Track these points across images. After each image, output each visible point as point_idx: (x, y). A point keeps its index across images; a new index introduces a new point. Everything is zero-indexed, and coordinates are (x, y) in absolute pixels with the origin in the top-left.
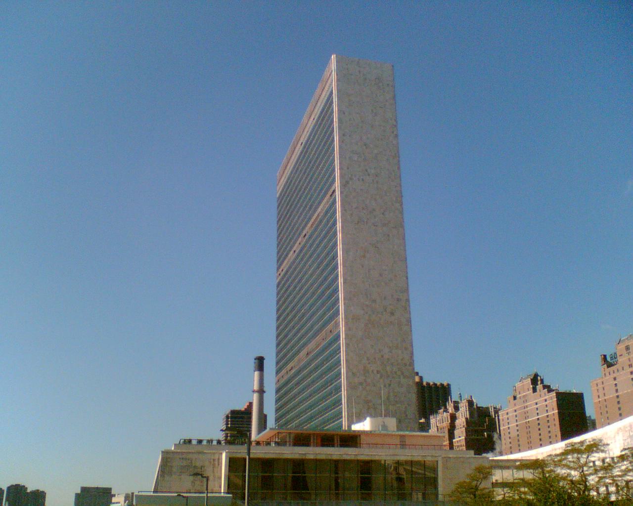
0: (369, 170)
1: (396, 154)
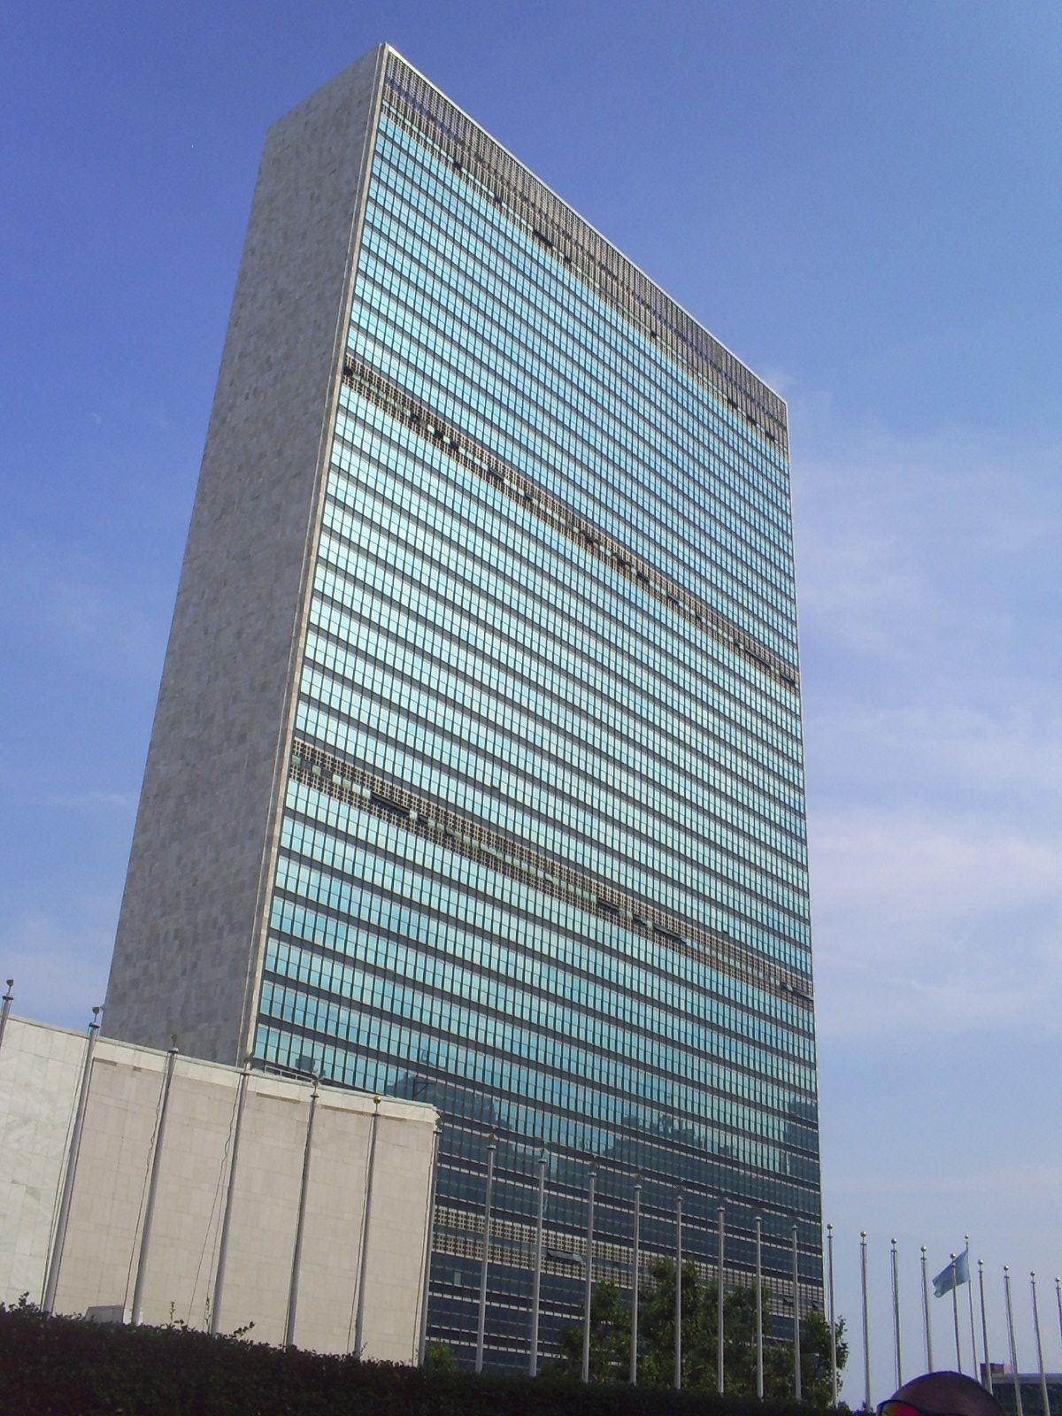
0: (272, 359)
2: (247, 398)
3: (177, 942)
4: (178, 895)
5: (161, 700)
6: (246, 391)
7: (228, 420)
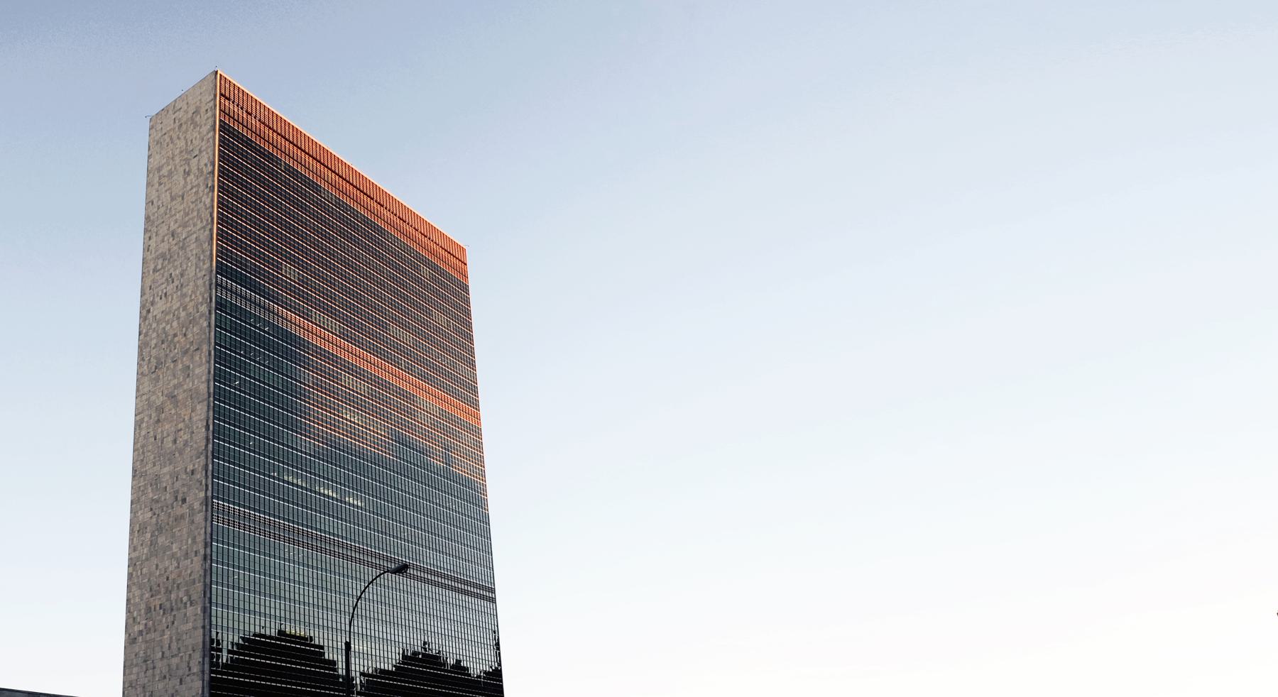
1: (207, 220)
2: (161, 298)
3: (162, 611)
4: (159, 586)
5: (134, 477)
6: (160, 294)
7: (151, 311)
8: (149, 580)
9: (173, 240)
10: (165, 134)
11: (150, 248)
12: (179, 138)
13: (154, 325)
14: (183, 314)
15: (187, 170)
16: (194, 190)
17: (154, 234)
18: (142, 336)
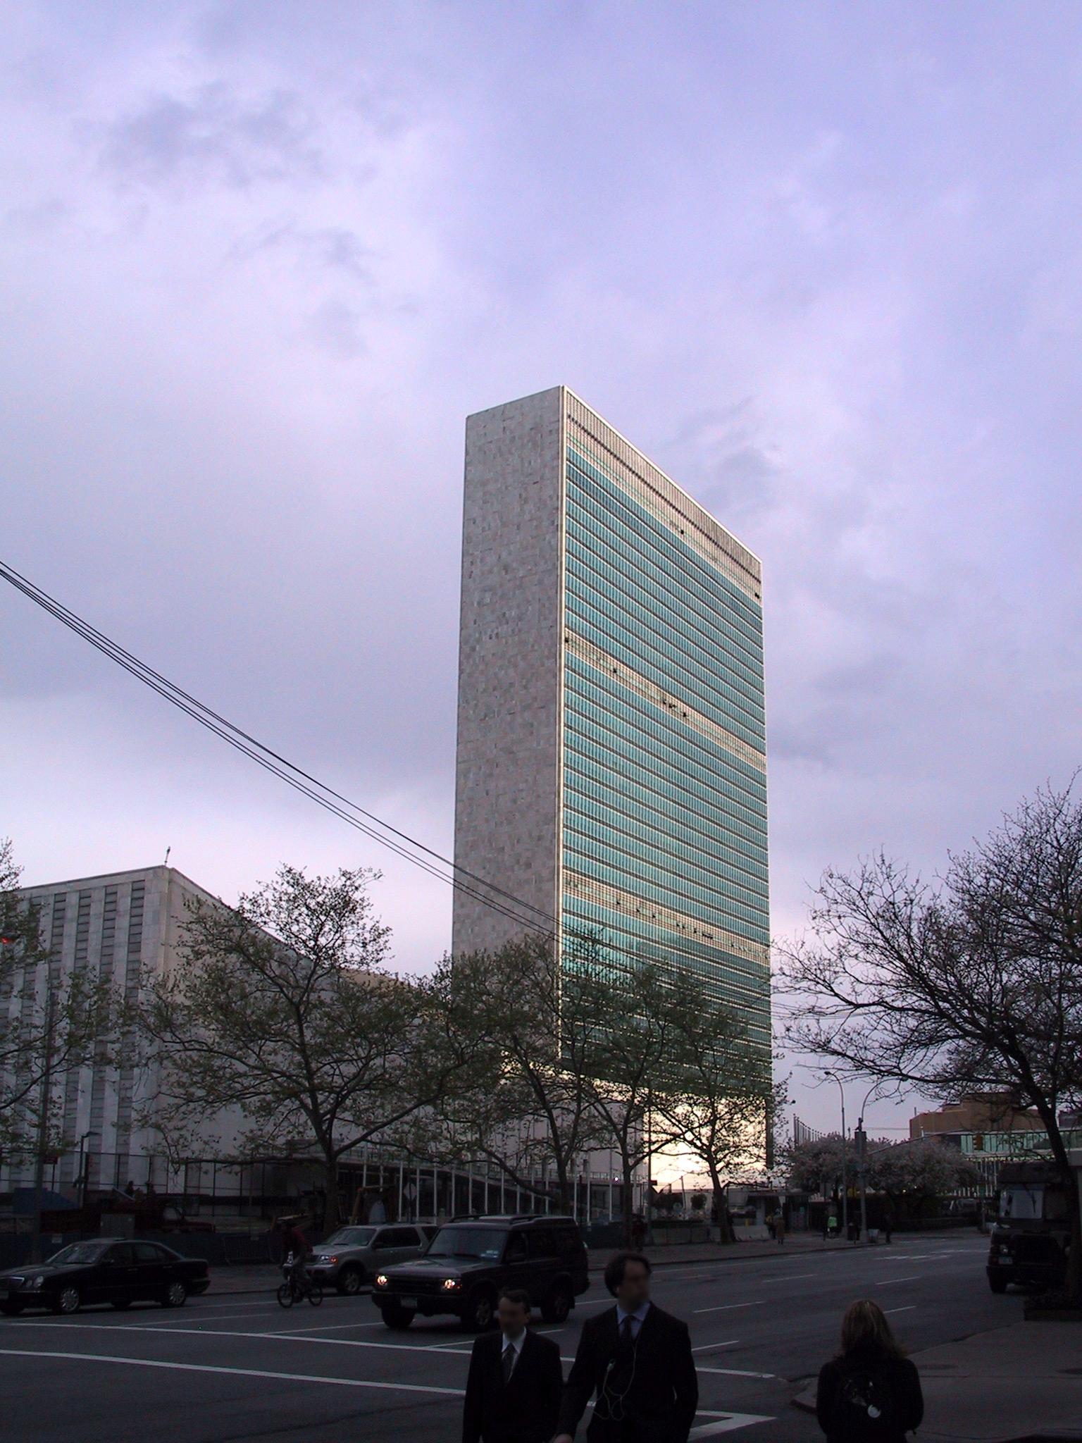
0: (507, 615)
2: (491, 638)
6: (489, 633)
7: (477, 649)
8: (483, 939)
9: (506, 573)
10: (491, 442)
11: (473, 575)
12: (512, 454)
13: (481, 667)
14: (522, 664)
15: (524, 496)
16: (535, 523)
17: (478, 560)
18: (464, 676)
